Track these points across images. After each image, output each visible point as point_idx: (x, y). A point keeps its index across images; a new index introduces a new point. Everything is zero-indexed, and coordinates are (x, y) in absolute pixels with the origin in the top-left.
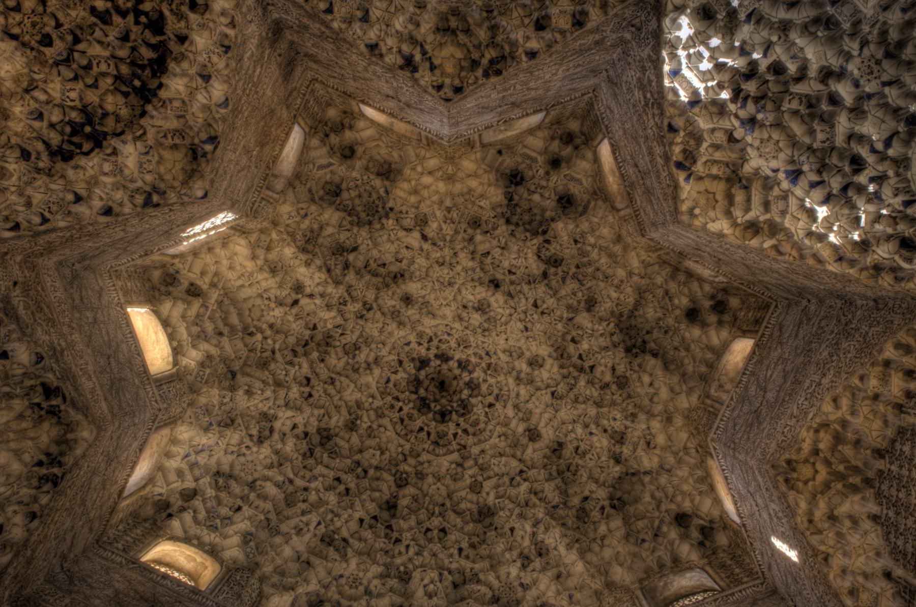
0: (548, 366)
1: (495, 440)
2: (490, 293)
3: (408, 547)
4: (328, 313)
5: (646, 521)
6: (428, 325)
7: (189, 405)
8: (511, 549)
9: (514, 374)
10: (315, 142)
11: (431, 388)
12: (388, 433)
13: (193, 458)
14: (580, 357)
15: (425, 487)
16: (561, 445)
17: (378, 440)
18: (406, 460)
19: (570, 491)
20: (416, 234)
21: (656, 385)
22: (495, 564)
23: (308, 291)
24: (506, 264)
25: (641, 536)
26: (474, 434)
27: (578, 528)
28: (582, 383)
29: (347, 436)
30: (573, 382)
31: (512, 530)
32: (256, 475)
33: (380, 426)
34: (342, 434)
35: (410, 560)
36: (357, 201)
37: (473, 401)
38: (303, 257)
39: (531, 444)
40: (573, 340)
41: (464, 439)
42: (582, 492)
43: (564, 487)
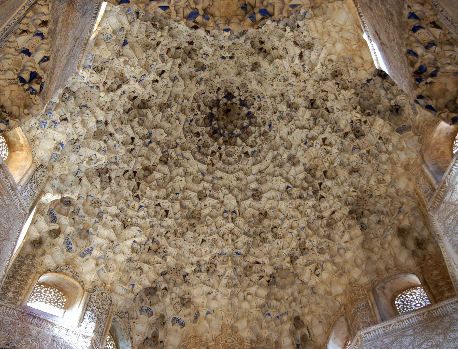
1: (233, 177)
6: (253, 86)
14: (320, 184)
15: (175, 172)
18: (176, 147)
19: (252, 250)
20: (297, 51)
21: (348, 245)
24: (329, 104)
25: (270, 311)
26: (224, 161)
27: (240, 276)
29: (156, 112)
31: (203, 241)
32: (89, 104)
33: (178, 119)
39: (251, 199)
40: (325, 172)
42: (258, 257)
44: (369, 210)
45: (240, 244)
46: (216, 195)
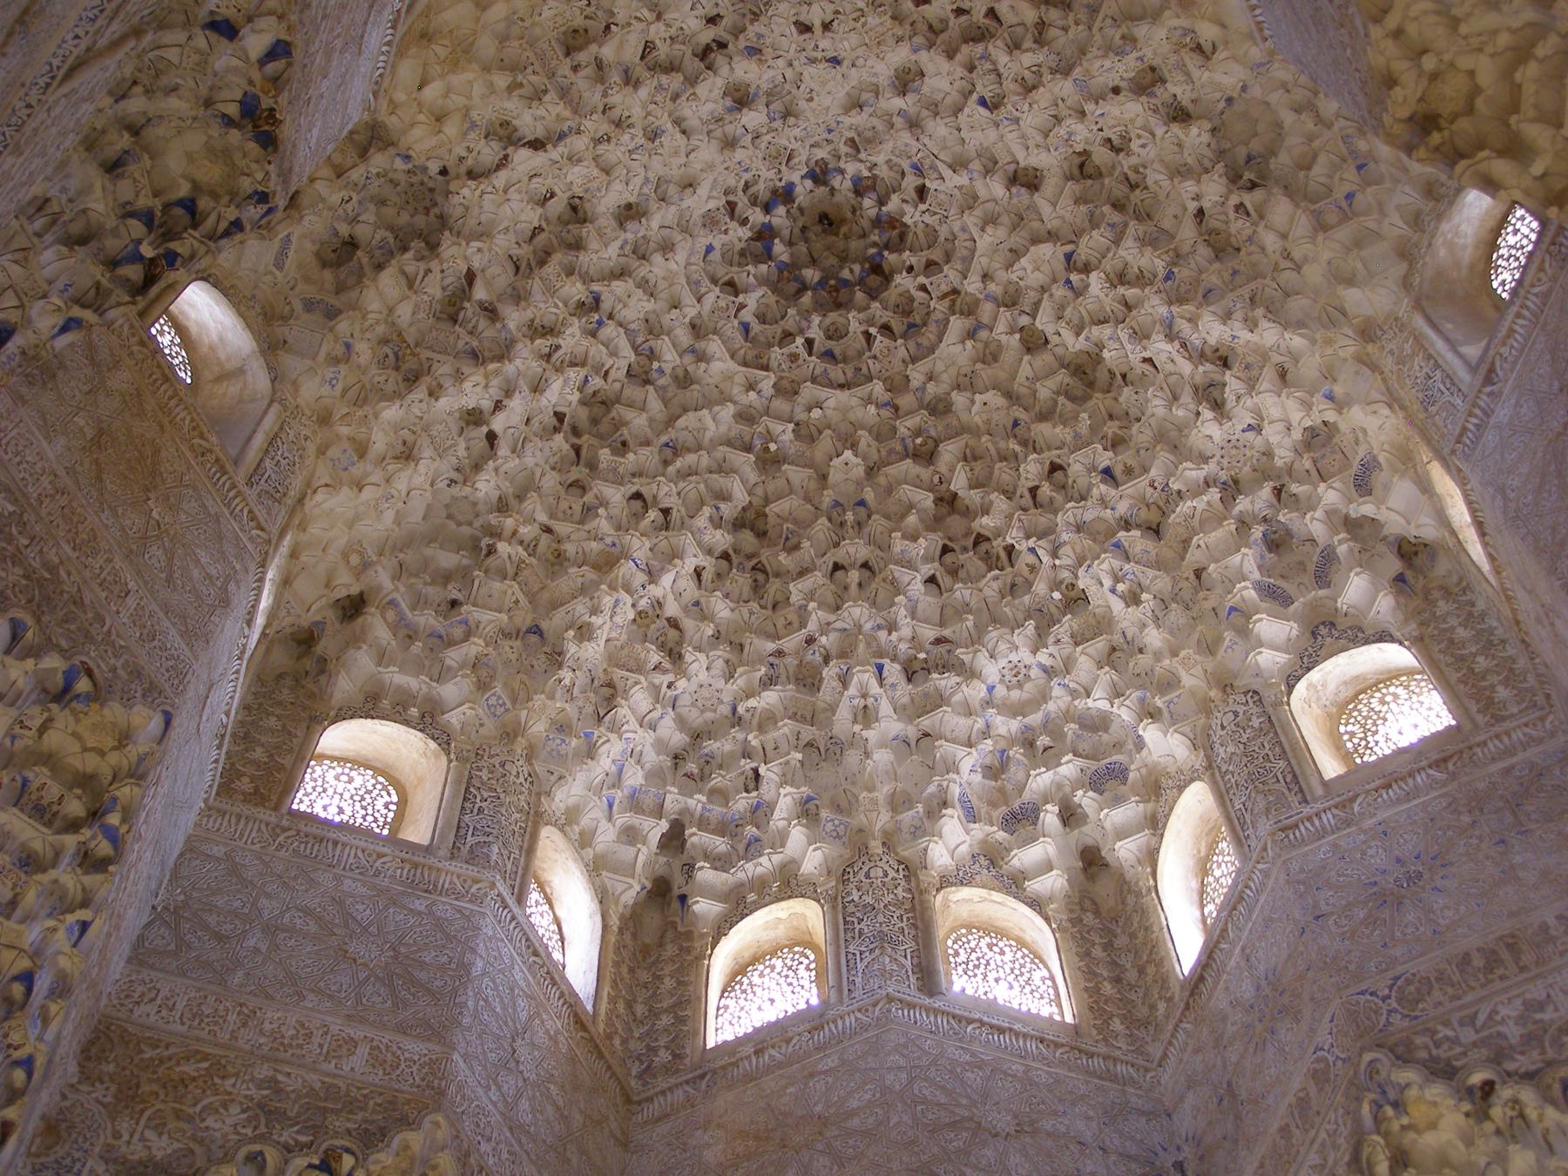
0: (929, 68)
1: (985, 241)
2: (725, 70)
5: (1322, 159)
6: (704, 200)
7: (529, 759)
8: (1175, 398)
11: (818, 246)
12: (831, 403)
15: (964, 417)
17: (828, 432)
18: (896, 408)
19: (1167, 224)
20: (524, 159)
22: (1174, 442)
23: (487, 405)
24: (693, 24)
26: (948, 258)
27: (1235, 273)
28: (1002, 59)
29: (781, 482)
30: (988, 66)
32: (727, 698)
34: (771, 487)
36: (389, 212)
38: (420, 392)
46: (1032, 295)
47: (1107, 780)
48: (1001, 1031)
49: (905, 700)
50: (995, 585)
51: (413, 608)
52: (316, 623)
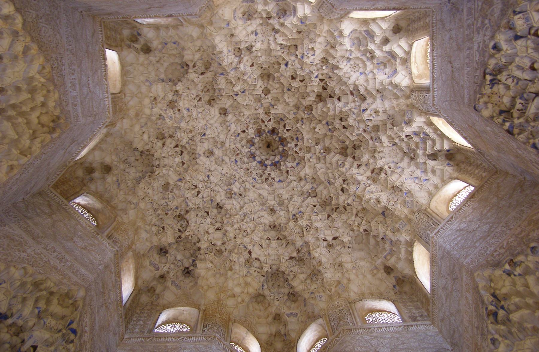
2: (223, 201)
3: (317, 77)
4: (318, 226)
5: (170, 53)
6: (265, 190)
9: (224, 148)
10: (293, 335)
11: (275, 146)
12: (307, 137)
13: (423, 177)
16: (209, 103)
19: (211, 79)
20: (254, 256)
21: (141, 132)
22: (269, 51)
23: (325, 243)
24: (209, 220)
25: (175, 46)
29: (331, 146)
35: (318, 70)
36: (281, 284)
37: (253, 136)
38: (321, 268)
41: (266, 118)
43: (214, 83)
44: (137, 160)
45: (223, 80)
47: (371, 35)
48: (433, 65)
49: (371, 99)
50: (331, 83)
51: (386, 251)
52: (395, 279)
